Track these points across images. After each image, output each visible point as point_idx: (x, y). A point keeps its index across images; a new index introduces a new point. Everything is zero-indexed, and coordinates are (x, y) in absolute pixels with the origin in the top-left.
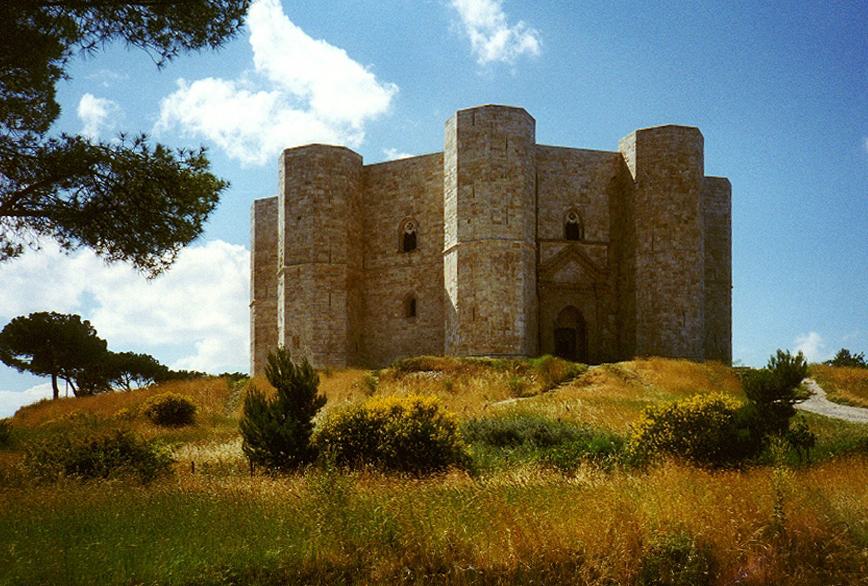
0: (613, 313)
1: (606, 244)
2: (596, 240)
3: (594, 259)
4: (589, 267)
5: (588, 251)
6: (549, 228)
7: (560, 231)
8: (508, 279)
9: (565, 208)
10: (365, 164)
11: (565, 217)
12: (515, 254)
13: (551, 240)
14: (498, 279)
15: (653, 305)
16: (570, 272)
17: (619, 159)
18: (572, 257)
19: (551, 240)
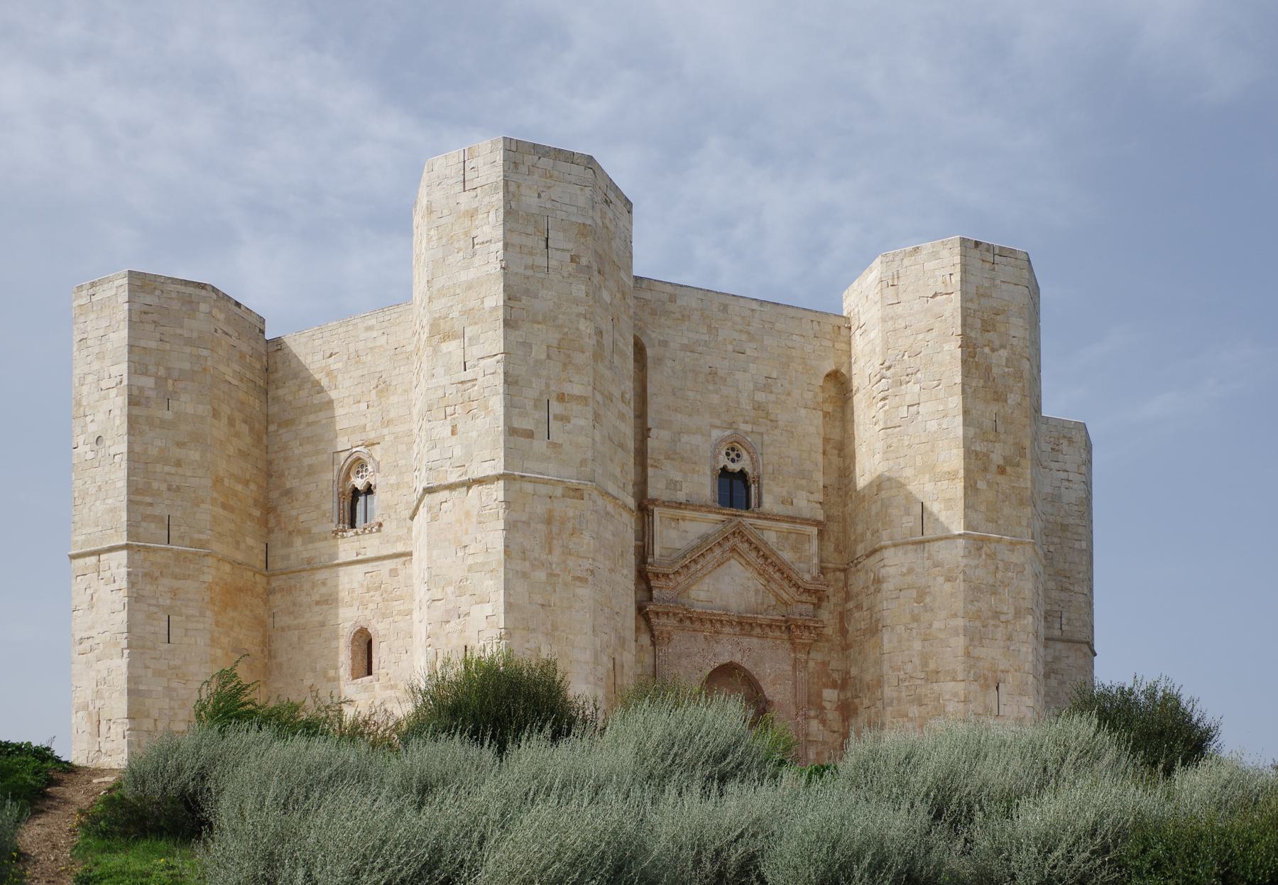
0: (834, 685)
1: (817, 523)
2: (789, 511)
3: (787, 555)
4: (777, 576)
5: (771, 537)
6: (677, 476)
7: (704, 486)
8: (551, 575)
9: (716, 434)
10: (269, 335)
11: (715, 457)
12: (571, 514)
13: (679, 505)
14: (525, 575)
15: (925, 664)
16: (730, 586)
17: (842, 328)
18: (733, 550)
19: (679, 505)
